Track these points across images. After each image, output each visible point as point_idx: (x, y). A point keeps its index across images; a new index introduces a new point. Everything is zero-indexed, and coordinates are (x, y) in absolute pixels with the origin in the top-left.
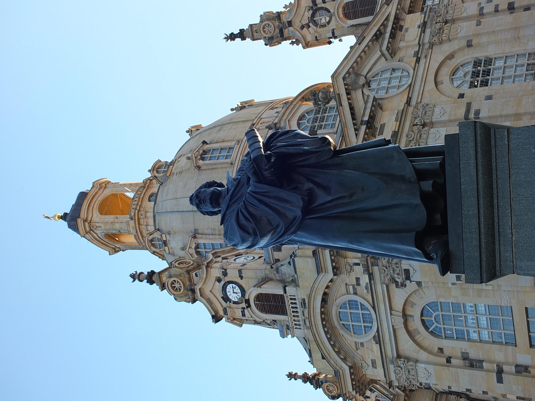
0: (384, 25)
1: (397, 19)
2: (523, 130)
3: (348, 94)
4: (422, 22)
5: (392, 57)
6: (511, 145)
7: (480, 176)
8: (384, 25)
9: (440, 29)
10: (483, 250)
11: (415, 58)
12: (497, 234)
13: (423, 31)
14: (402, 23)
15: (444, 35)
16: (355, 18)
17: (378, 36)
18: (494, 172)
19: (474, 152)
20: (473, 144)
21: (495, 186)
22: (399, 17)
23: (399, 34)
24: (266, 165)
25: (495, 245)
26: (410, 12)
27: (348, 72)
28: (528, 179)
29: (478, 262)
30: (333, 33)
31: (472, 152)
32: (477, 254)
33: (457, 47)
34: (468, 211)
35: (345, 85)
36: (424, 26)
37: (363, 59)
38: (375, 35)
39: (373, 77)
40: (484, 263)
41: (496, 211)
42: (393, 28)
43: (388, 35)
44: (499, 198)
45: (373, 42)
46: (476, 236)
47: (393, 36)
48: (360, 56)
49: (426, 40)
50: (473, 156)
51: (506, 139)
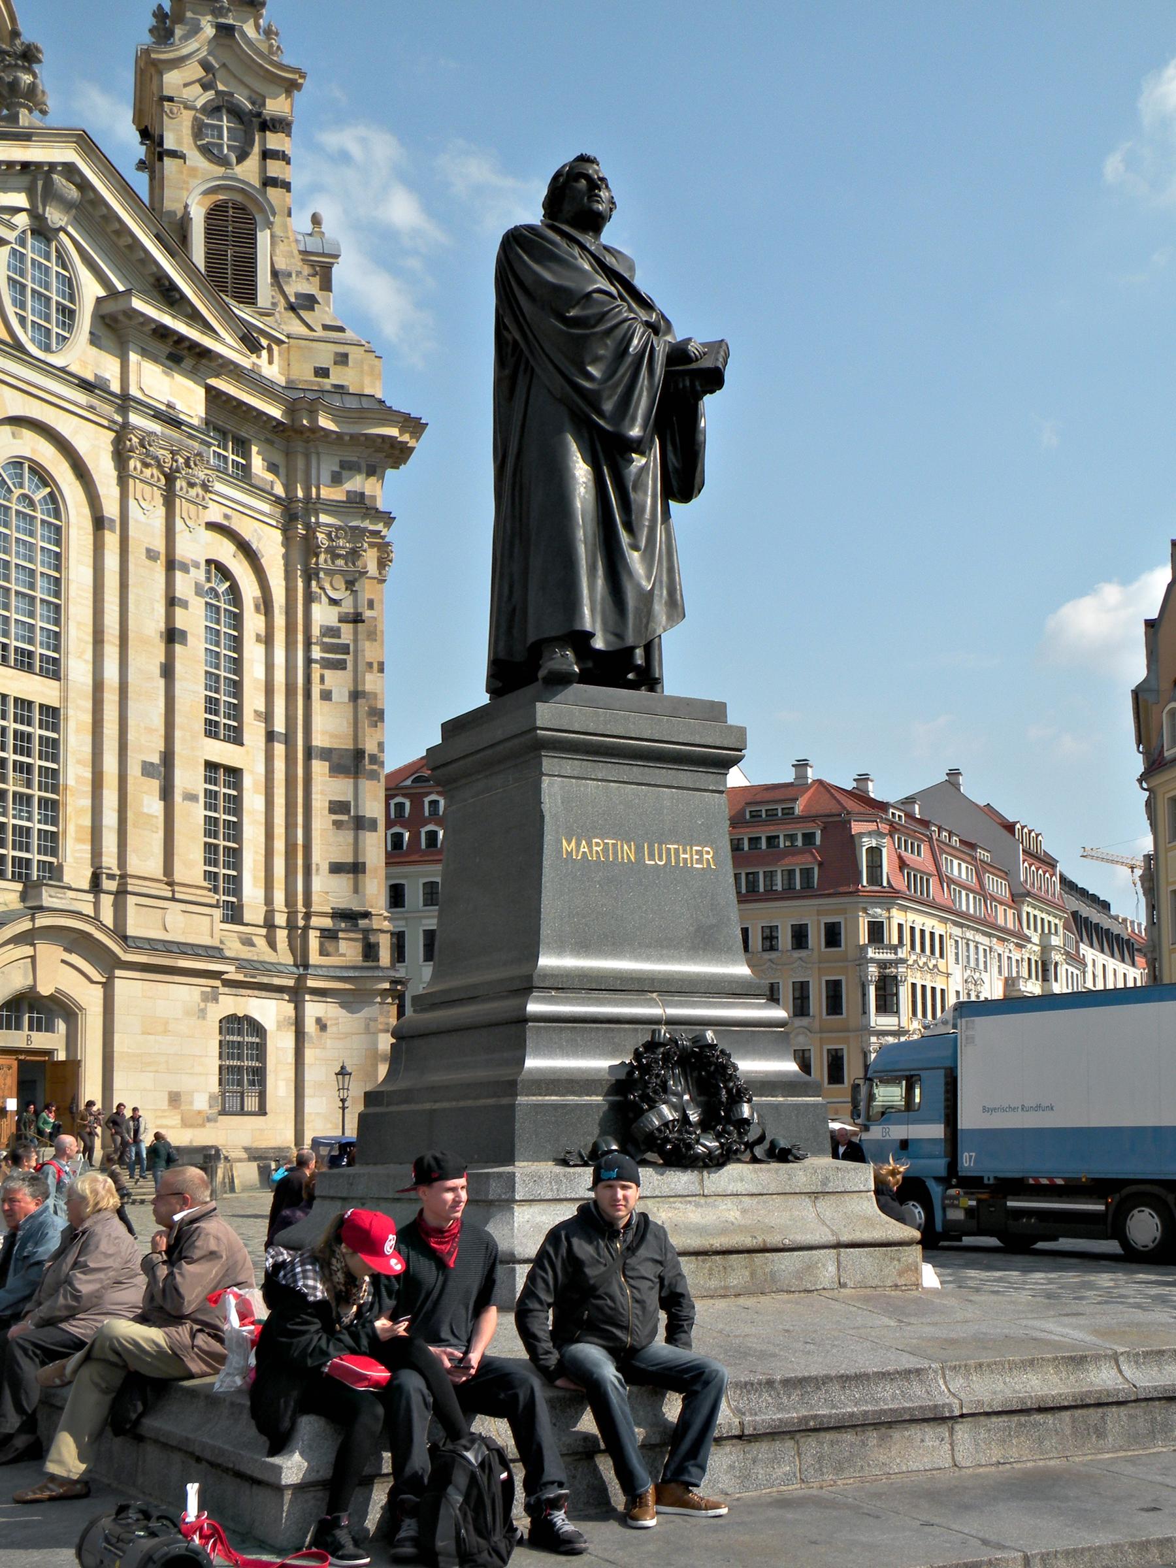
0: (194, 317)
1: (204, 353)
3: (25, 165)
4: (182, 416)
5: (103, 317)
8: (194, 317)
9: (156, 458)
11: (90, 377)
13: (158, 415)
14: (188, 362)
15: (139, 465)
16: (210, 233)
17: (168, 294)
22: (204, 361)
23: (165, 349)
26: (209, 389)
27: (84, 185)
30: (174, 154)
33: (102, 490)
35: (52, 166)
36: (169, 418)
37: (114, 238)
38: (173, 287)
39: (57, 251)
42: (182, 339)
43: (167, 320)
45: (153, 274)
47: (162, 332)
48: (124, 230)
49: (134, 419)
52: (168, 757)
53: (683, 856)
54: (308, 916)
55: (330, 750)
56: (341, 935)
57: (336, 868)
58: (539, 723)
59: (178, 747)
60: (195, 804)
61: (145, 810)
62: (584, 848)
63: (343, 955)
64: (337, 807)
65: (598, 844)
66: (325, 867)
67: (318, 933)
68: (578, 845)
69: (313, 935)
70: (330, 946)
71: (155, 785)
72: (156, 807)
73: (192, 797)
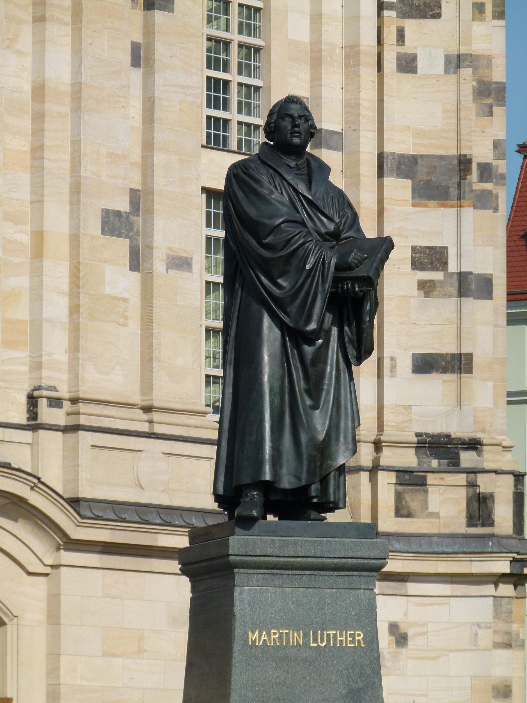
2: (373, 604)
6: (359, 591)
7: (335, 560)
10: (262, 559)
12: (275, 571)
18: (335, 573)
19: (359, 556)
20: (366, 556)
21: (322, 573)
24: (359, 288)
25: (264, 569)
28: (327, 606)
29: (251, 553)
31: (359, 554)
32: (258, 552)
34: (301, 546)
40: (249, 558)
41: (298, 572)
44: (309, 577)
46: (276, 552)
50: (354, 555)
51: (366, 587)
52: (140, 200)
53: (343, 639)
54: (378, 446)
55: (414, 159)
56: (431, 479)
57: (425, 364)
58: (231, 552)
59: (159, 183)
60: (185, 275)
61: (108, 290)
62: (264, 637)
63: (436, 515)
64: (429, 258)
65: (275, 634)
66: (405, 363)
67: (392, 478)
68: (260, 635)
69: (386, 481)
70: (413, 501)
71: (121, 246)
72: (121, 282)
73: (181, 263)
